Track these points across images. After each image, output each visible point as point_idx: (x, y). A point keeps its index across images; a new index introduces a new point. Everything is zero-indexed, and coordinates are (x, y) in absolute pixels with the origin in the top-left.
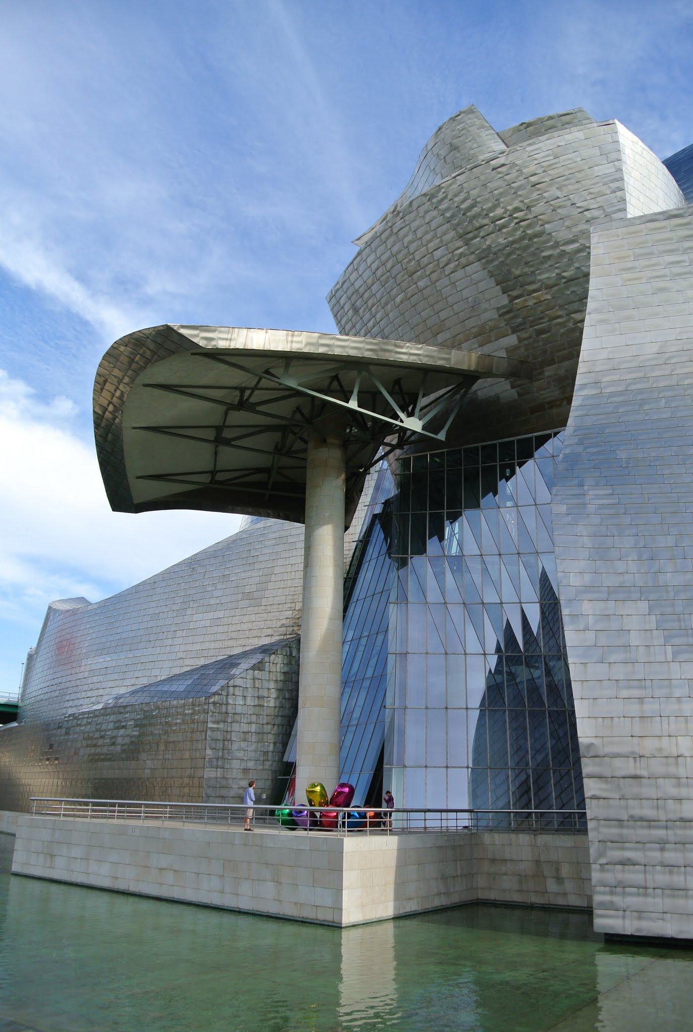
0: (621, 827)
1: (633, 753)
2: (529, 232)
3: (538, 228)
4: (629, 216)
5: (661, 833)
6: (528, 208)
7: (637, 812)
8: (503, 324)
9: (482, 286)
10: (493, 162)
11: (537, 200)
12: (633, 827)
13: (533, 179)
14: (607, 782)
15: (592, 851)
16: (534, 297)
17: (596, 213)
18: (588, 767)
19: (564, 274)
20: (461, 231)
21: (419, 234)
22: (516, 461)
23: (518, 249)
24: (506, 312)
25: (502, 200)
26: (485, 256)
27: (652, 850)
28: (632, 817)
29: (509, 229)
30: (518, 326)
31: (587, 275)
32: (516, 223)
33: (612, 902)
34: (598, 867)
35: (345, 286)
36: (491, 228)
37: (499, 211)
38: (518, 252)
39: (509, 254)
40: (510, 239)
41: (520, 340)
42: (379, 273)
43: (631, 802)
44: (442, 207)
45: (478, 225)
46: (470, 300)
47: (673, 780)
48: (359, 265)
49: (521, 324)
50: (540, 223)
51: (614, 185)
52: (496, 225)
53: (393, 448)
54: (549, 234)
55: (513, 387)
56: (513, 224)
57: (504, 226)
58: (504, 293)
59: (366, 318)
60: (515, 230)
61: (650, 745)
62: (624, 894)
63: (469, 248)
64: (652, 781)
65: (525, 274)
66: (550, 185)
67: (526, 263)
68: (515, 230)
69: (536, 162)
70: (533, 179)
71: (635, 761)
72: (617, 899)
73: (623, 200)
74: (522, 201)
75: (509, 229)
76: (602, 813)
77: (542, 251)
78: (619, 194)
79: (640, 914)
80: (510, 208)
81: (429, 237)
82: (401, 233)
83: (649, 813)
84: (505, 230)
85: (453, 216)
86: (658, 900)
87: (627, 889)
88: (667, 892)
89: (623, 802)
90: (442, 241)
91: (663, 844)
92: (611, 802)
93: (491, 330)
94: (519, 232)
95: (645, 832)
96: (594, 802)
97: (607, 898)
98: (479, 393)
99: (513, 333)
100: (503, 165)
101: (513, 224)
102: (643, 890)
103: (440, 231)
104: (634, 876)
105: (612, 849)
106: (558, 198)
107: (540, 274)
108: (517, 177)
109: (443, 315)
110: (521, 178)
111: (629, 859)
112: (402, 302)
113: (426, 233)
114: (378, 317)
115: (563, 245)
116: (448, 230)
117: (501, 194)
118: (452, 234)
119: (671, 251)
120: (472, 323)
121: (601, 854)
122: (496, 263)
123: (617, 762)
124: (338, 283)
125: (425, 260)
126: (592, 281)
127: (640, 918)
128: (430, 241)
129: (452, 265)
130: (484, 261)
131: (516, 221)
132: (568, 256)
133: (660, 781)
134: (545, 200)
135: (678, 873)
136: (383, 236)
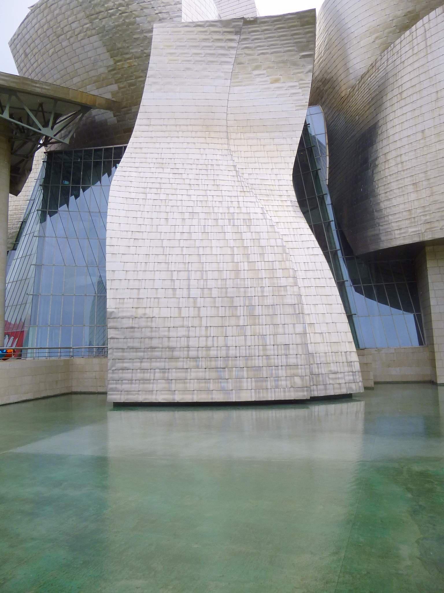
0: (123, 352)
1: (132, 316)
2: (127, 21)
3: (132, 20)
4: (183, 21)
5: (141, 354)
6: (128, 5)
7: (131, 345)
8: (110, 77)
9: (100, 51)
12: (129, 352)
14: (118, 330)
15: (109, 364)
16: (128, 63)
17: (165, 16)
18: (110, 323)
19: (145, 51)
20: (88, 13)
21: (63, 10)
22: (103, 160)
23: (120, 31)
24: (113, 70)
26: (102, 32)
27: (136, 362)
28: (128, 347)
30: (119, 79)
31: (149, 55)
32: (120, 14)
33: (116, 388)
34: (111, 371)
35: (20, 37)
36: (105, 14)
38: (120, 33)
39: (115, 33)
40: (116, 23)
41: (120, 88)
42: (39, 32)
43: (129, 340)
46: (92, 59)
47: (149, 329)
48: (27, 25)
49: (120, 78)
50: (134, 16)
53: (42, 145)
55: (114, 116)
56: (118, 14)
57: (113, 14)
58: (111, 57)
59: (32, 61)
60: (119, 18)
61: (140, 312)
62: (122, 384)
63: (92, 25)
64: (140, 329)
65: (124, 48)
67: (125, 41)
68: (119, 18)
71: (133, 320)
72: (119, 386)
73: (180, 10)
76: (115, 346)
77: (134, 35)
78: (178, 6)
79: (128, 392)
80: (117, 3)
81: (69, 13)
82: (53, 7)
83: (136, 344)
84: (113, 17)
86: (137, 385)
87: (124, 381)
88: (142, 381)
89: (125, 340)
90: (76, 18)
91: (141, 360)
92: (120, 340)
93: (103, 80)
94: (121, 20)
95: (135, 354)
96: (112, 340)
97: (114, 386)
98: (96, 117)
99: (116, 83)
101: (118, 14)
102: (131, 381)
103: (75, 10)
104: (128, 375)
105: (119, 363)
107: (131, 49)
109: (77, 66)
111: (126, 368)
112: (52, 54)
113: (67, 11)
114: (39, 62)
115: (145, 33)
116: (80, 11)
118: (82, 14)
119: (195, 46)
120: (92, 73)
121: (113, 366)
122: (107, 37)
123: (125, 321)
124: (15, 35)
125: (66, 29)
126: (152, 58)
127: (128, 394)
128: (69, 16)
129: (82, 35)
130: (100, 35)
131: (120, 12)
132: (148, 40)
133: (144, 329)
135: (147, 373)
136: (42, 7)
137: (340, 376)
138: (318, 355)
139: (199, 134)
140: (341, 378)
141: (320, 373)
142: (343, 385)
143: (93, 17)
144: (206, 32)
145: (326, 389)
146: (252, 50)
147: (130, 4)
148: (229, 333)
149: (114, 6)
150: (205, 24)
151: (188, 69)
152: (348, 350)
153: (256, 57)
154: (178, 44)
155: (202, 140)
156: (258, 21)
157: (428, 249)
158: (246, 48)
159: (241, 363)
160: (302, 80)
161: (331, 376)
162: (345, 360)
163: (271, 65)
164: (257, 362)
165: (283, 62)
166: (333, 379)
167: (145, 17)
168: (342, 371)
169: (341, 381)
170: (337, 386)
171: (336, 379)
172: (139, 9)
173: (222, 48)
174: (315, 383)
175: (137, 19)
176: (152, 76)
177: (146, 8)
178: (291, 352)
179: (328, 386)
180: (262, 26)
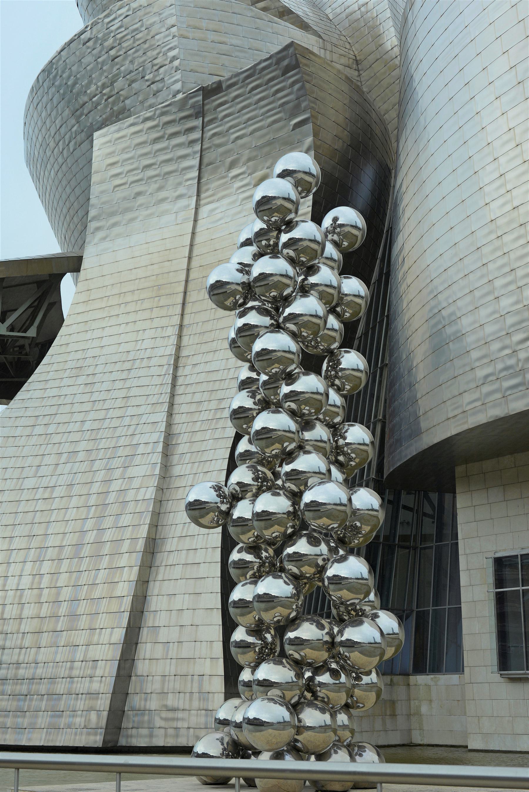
2: (115, 108)
3: (121, 105)
6: (112, 84)
10: (82, 37)
11: (117, 75)
13: (113, 53)
25: (93, 76)
29: (102, 105)
32: (106, 100)
37: (93, 88)
40: (104, 116)
44: (57, 83)
45: (81, 102)
50: (122, 98)
52: (93, 102)
54: (129, 110)
57: (98, 104)
60: (106, 106)
66: (125, 59)
69: (112, 35)
70: (113, 53)
74: (107, 77)
75: (102, 105)
78: (176, 63)
80: (100, 84)
84: (99, 108)
85: (64, 94)
100: (89, 40)
101: (103, 102)
106: (131, 72)
108: (101, 51)
110: (103, 53)
117: (92, 70)
118: (67, 112)
119: (146, 154)
129: (72, 143)
131: (105, 97)
134: (122, 75)
137: (180, 715)
138: (150, 678)
140: (183, 719)
141: (147, 707)
142: (183, 732)
143: (78, 113)
145: (151, 736)
146: (224, 136)
147: (115, 81)
148: (43, 644)
149: (97, 89)
150: (155, 114)
151: (139, 194)
152: (208, 671)
153: (230, 146)
155: (146, 315)
156: (224, 86)
157: (459, 470)
158: (214, 135)
159: (43, 688)
161: (164, 714)
162: (195, 689)
163: (254, 154)
164: (61, 687)
165: (269, 143)
166: (166, 719)
167: (136, 95)
168: (187, 707)
169: (180, 724)
170: (171, 731)
171: (173, 719)
172: (127, 86)
173: (180, 145)
174: (136, 725)
175: (127, 102)
176: (94, 218)
177: (133, 81)
178: (99, 672)
179: (156, 732)
180: (230, 93)
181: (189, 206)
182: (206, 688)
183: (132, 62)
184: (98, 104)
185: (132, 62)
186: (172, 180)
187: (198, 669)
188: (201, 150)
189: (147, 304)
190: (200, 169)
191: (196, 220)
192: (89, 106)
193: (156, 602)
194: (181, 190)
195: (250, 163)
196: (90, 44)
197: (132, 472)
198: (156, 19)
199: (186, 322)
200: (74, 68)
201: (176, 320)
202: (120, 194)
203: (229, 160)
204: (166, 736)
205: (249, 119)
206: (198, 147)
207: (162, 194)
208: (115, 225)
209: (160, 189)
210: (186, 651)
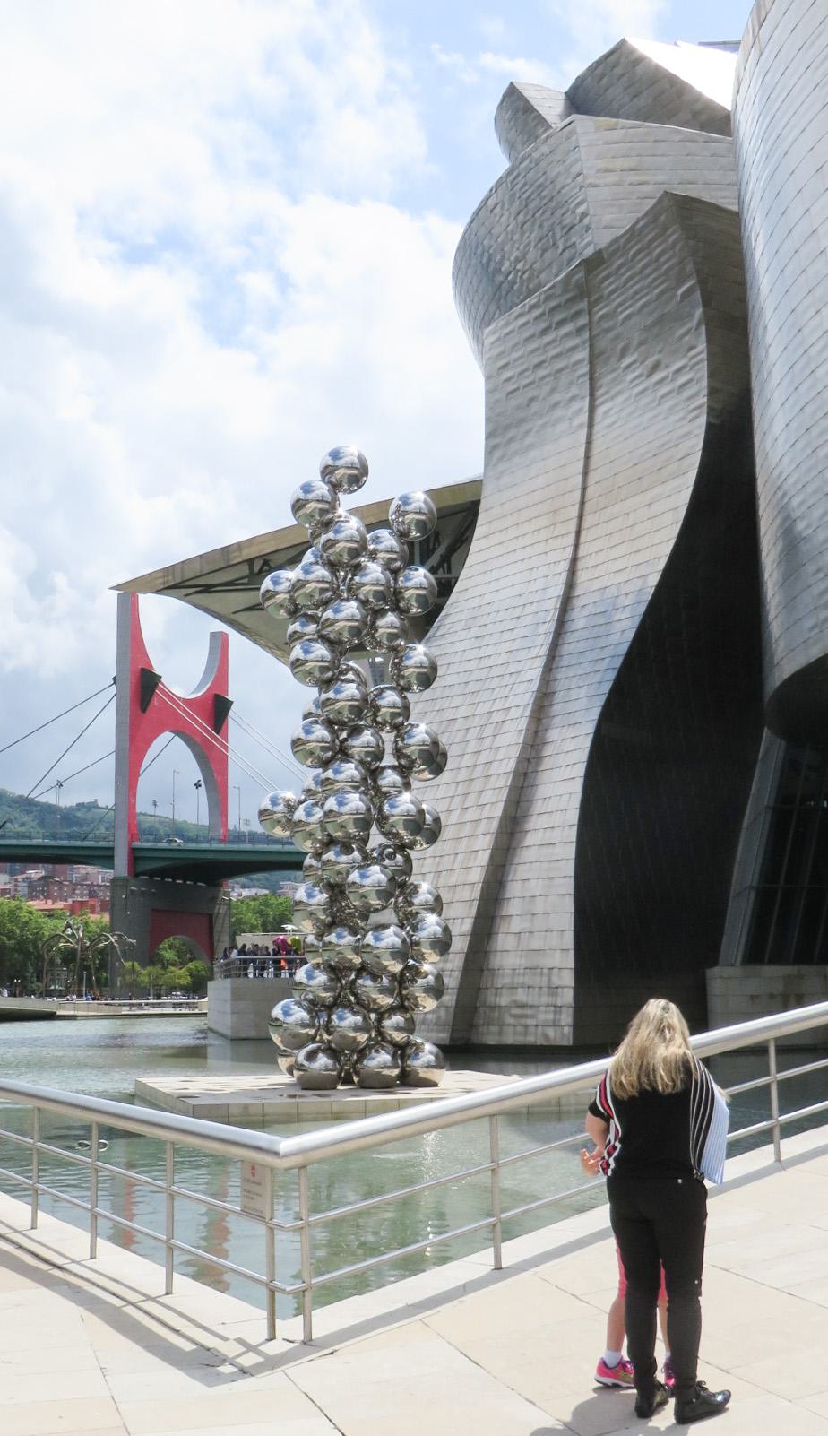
37: (507, 264)
51: (580, 210)
57: (514, 283)
137: (529, 1012)
139: (543, 535)
140: (532, 1017)
142: (532, 1029)
144: (542, 314)
145: (500, 1033)
151: (532, 400)
153: (619, 330)
154: (515, 355)
155: (540, 548)
158: (603, 317)
160: (691, 348)
162: (544, 984)
166: (516, 1016)
169: (529, 1022)
170: (519, 1029)
181: (581, 410)
182: (556, 981)
183: (541, 226)
184: (514, 283)
185: (541, 226)
186: (564, 379)
187: (548, 962)
188: (591, 338)
189: (543, 535)
190: (591, 363)
191: (591, 425)
192: (505, 285)
193: (514, 889)
194: (574, 390)
195: (642, 348)
196: (498, 209)
197: (500, 741)
198: (560, 168)
199: (580, 554)
200: (486, 242)
201: (569, 552)
202: (514, 402)
203: (620, 347)
204: (515, 1033)
205: (636, 293)
206: (586, 335)
207: (557, 397)
208: (511, 440)
209: (553, 391)
210: (536, 943)
